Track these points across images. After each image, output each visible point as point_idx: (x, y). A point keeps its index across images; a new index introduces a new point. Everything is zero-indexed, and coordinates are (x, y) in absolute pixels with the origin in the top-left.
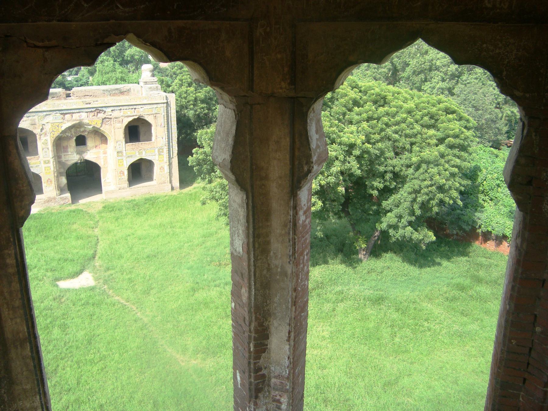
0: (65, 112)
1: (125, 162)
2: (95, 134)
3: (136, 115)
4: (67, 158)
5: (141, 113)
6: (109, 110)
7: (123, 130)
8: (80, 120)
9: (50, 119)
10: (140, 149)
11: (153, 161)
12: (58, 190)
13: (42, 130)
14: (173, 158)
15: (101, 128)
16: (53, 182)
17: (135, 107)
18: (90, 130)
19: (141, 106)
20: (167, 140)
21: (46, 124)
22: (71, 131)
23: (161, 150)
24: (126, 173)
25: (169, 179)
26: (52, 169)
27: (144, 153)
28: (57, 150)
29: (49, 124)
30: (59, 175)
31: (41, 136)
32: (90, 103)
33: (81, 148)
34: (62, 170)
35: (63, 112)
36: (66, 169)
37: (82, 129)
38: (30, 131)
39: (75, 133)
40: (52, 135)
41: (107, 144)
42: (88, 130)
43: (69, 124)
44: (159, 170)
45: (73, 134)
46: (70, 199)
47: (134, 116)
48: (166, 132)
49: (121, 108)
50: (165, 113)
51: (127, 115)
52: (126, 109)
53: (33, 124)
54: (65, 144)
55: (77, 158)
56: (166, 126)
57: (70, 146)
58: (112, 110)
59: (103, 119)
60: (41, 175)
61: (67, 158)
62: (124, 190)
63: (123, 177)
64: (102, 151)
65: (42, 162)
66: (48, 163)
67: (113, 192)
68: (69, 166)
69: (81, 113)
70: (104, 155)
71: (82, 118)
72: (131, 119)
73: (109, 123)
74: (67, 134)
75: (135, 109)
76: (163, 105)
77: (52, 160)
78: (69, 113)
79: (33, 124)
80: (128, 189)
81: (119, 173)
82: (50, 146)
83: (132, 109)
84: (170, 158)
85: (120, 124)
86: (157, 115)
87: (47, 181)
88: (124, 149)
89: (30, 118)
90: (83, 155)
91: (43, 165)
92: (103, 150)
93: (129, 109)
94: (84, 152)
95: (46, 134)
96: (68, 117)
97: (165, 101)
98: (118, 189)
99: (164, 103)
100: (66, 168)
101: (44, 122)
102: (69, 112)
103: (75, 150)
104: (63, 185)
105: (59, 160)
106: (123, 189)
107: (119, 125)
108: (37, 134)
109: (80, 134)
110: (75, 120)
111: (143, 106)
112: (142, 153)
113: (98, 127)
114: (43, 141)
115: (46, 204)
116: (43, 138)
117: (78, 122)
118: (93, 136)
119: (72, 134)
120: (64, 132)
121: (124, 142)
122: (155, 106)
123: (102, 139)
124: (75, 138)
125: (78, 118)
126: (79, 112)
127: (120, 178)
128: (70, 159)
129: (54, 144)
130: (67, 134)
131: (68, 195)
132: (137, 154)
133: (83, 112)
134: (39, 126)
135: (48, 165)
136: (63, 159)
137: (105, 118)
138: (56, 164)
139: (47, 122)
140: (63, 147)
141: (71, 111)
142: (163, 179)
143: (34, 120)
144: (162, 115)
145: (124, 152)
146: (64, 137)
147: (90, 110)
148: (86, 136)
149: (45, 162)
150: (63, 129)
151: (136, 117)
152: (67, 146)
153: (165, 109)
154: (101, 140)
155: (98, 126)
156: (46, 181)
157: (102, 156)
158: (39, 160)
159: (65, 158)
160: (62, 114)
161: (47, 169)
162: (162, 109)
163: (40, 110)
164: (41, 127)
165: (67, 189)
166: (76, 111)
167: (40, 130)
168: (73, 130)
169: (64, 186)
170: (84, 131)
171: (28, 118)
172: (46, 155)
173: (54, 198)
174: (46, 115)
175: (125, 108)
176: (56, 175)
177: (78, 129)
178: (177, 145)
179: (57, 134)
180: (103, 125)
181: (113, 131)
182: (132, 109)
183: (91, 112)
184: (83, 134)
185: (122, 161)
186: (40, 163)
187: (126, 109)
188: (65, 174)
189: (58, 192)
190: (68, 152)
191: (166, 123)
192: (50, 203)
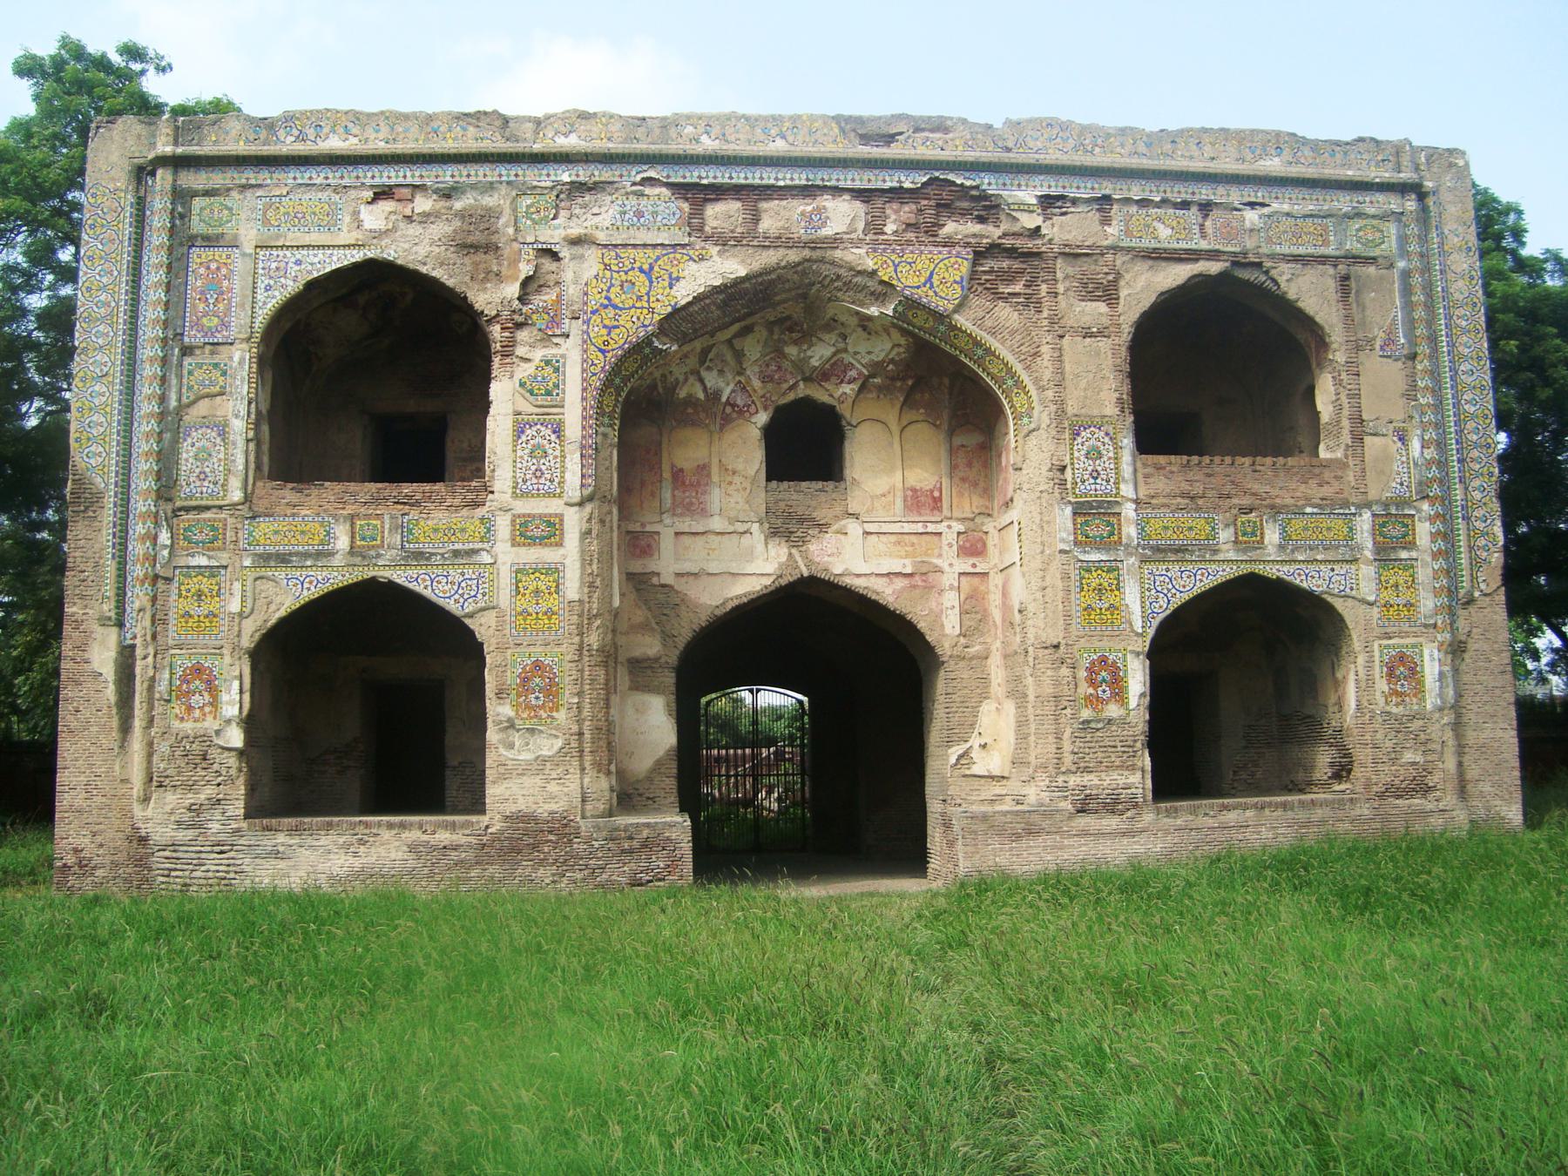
0: (708, 175)
1: (1132, 597)
2: (908, 403)
3: (1213, 255)
4: (696, 556)
5: (1250, 244)
6: (1026, 193)
7: (1124, 352)
8: (813, 244)
9: (601, 217)
10: (1246, 501)
11: (1338, 604)
12: (598, 766)
13: (529, 285)
14: (1470, 601)
15: (961, 320)
16: (568, 697)
17: (1204, 193)
18: (876, 368)
19: (1250, 194)
20: (1430, 453)
21: (565, 253)
22: (739, 355)
23: (1395, 531)
24: (1137, 681)
25: (1451, 764)
26: (573, 588)
27: (1272, 536)
28: (625, 488)
29: (592, 254)
30: (623, 678)
31: (522, 335)
32: (890, 139)
33: (802, 495)
34: (650, 646)
35: (693, 175)
36: (681, 646)
37: (819, 354)
38: (450, 291)
39: (766, 379)
40: (597, 333)
41: (987, 492)
42: (859, 368)
43: (729, 267)
44: (1382, 685)
45: (757, 383)
46: (686, 847)
47: (1192, 256)
48: (1425, 400)
49: (1106, 188)
50: (1416, 263)
51: (1147, 243)
52: (1144, 203)
53: (474, 248)
54: (688, 450)
55: (771, 568)
56: (1424, 349)
57: (724, 469)
58: (1048, 203)
59: (979, 256)
60: (484, 628)
61: (696, 556)
62: (1112, 822)
63: (1113, 710)
64: (951, 531)
65: (503, 526)
66: (534, 541)
67: (1028, 826)
68: (703, 619)
69: (827, 201)
70: (965, 565)
71: (827, 231)
72: (1175, 275)
73: (1018, 288)
74: (712, 380)
75: (1206, 207)
76: (1393, 203)
77: (574, 522)
78: (737, 191)
79: (474, 248)
80: (1148, 817)
81: (1083, 674)
82: (573, 415)
83: (1185, 205)
84: (1457, 601)
85: (1102, 307)
86: (1358, 269)
87: (525, 680)
88: (1127, 490)
89: (458, 205)
90: (813, 547)
91: (506, 554)
92: (958, 527)
93: (1164, 202)
94: (823, 527)
95: (555, 321)
96: (720, 214)
97: (1406, 176)
98: (1067, 805)
99: (1402, 189)
100: (685, 631)
101: (554, 234)
102: (740, 177)
103: (760, 499)
104: (642, 764)
105: (637, 566)
106: (1113, 805)
107: (1097, 310)
108: (492, 320)
109: (803, 390)
110: (777, 242)
111: (1260, 195)
112: (1257, 532)
113: (943, 306)
114: (524, 371)
115: (494, 870)
116: (531, 352)
117: (793, 256)
118: (892, 417)
119: (743, 388)
120: (679, 322)
121: (1128, 442)
122: (1343, 202)
123: (957, 441)
124: (763, 418)
125: (800, 232)
126: (808, 191)
127: (1086, 714)
128: (713, 567)
129: (609, 401)
130: (712, 380)
131: (677, 826)
132: (1225, 535)
133: (837, 191)
134: (514, 262)
135: (548, 555)
136: (667, 564)
137: (994, 250)
138: (605, 558)
139: (575, 231)
140: (678, 475)
141: (755, 177)
142: (1409, 756)
143: (490, 215)
144: (1396, 274)
145: (1129, 510)
146: (690, 401)
147: (890, 181)
148: (844, 410)
149: (525, 532)
150: (684, 293)
151: (1214, 268)
152: (703, 469)
153: (1413, 229)
154: (952, 452)
155: (943, 297)
156: (512, 678)
157: (951, 565)
158: (480, 512)
159: (677, 559)
160: (681, 189)
161: (530, 583)
162: (1392, 229)
163: (537, 147)
164: (525, 270)
165: (673, 798)
166: (785, 177)
167: (512, 290)
168: (753, 349)
169: (659, 764)
170: (832, 371)
171: (442, 203)
172: (538, 474)
173: (562, 828)
174: (579, 188)
175: (1136, 191)
176: (594, 640)
177: (792, 351)
178: (1496, 506)
179: (632, 326)
180: (975, 301)
181: (1045, 349)
182: (1185, 205)
183: (897, 194)
184: (821, 396)
185: (1106, 579)
186: (488, 535)
187: (1144, 203)
188: (670, 679)
189: (601, 786)
190: (704, 513)
191: (1421, 331)
192: (525, 868)
